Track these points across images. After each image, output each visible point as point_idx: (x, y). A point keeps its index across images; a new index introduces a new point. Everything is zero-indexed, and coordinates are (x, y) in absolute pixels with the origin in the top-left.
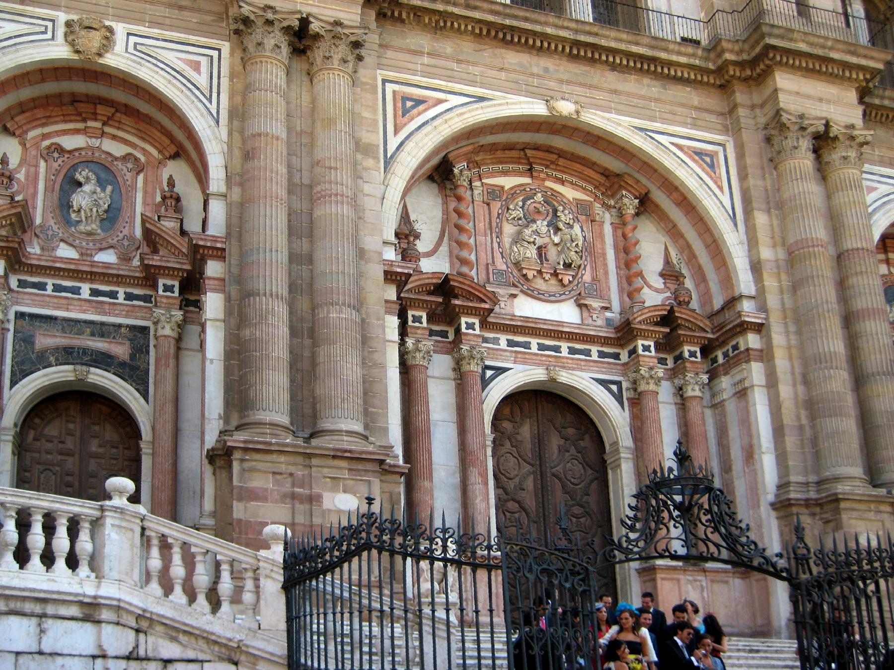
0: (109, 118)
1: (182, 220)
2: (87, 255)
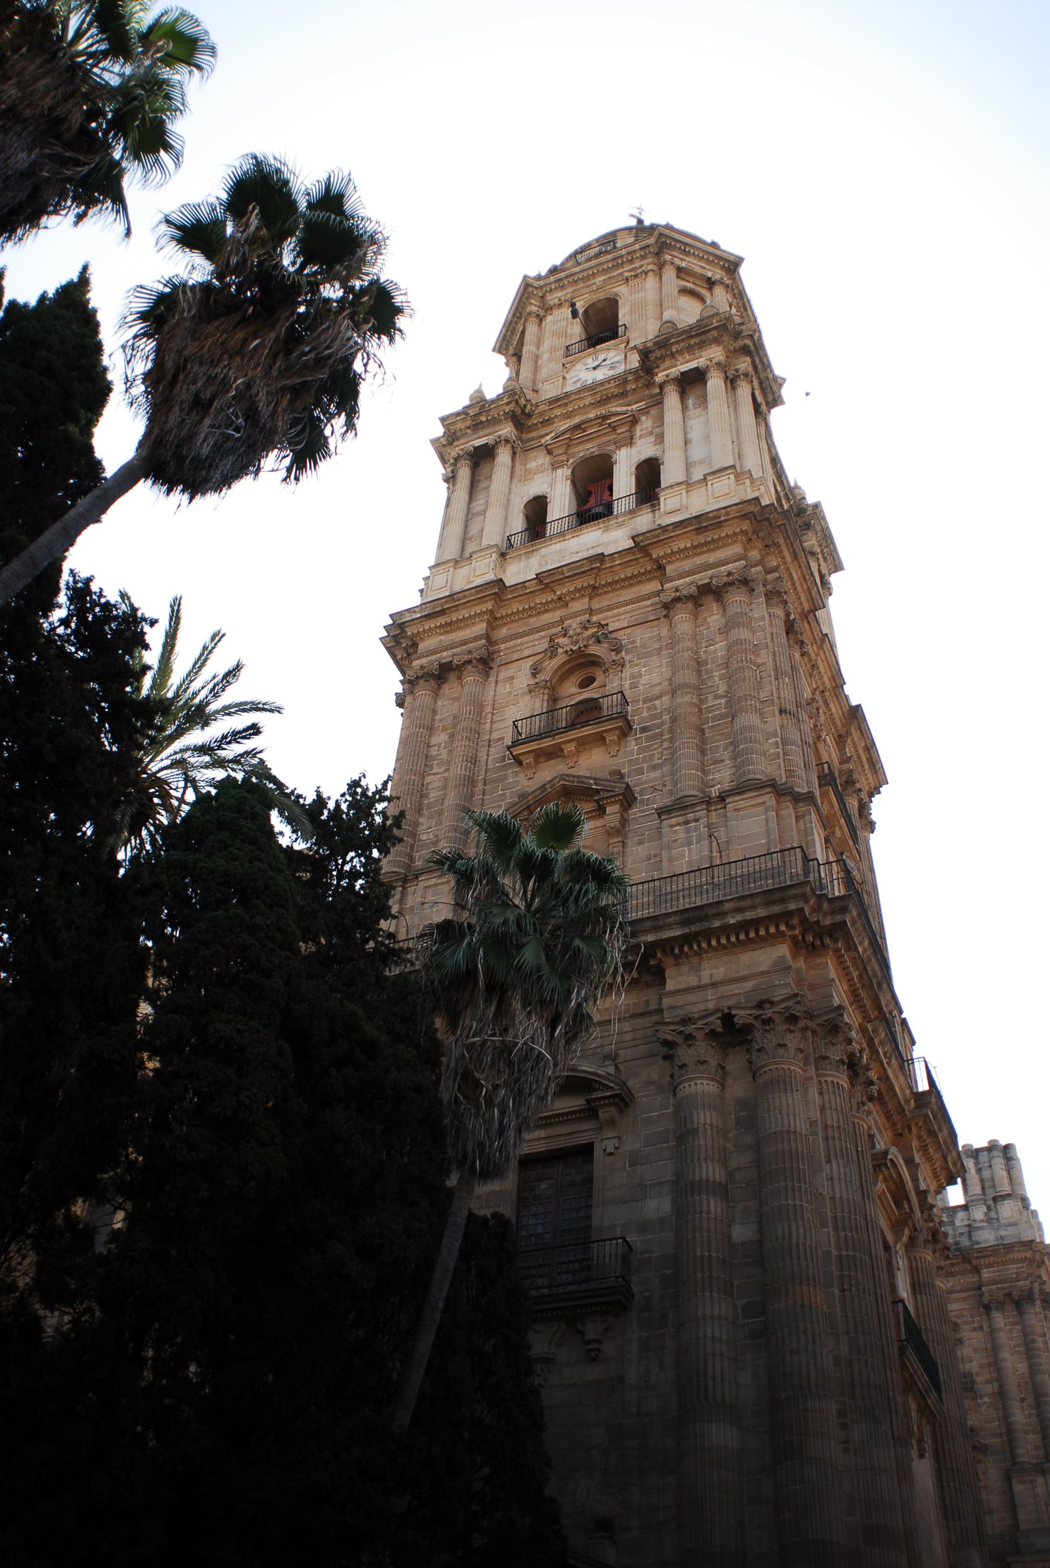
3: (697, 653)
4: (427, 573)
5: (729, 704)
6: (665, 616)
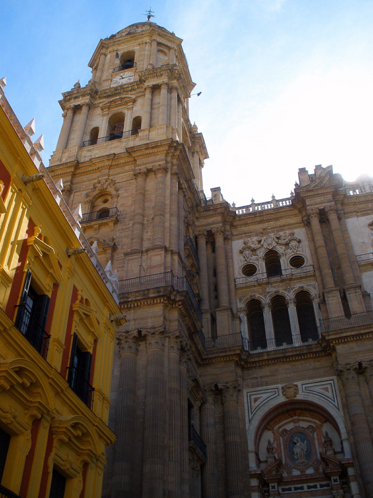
0: (300, 414)
1: (334, 450)
2: (303, 472)
4: (52, 154)
6: (135, 179)
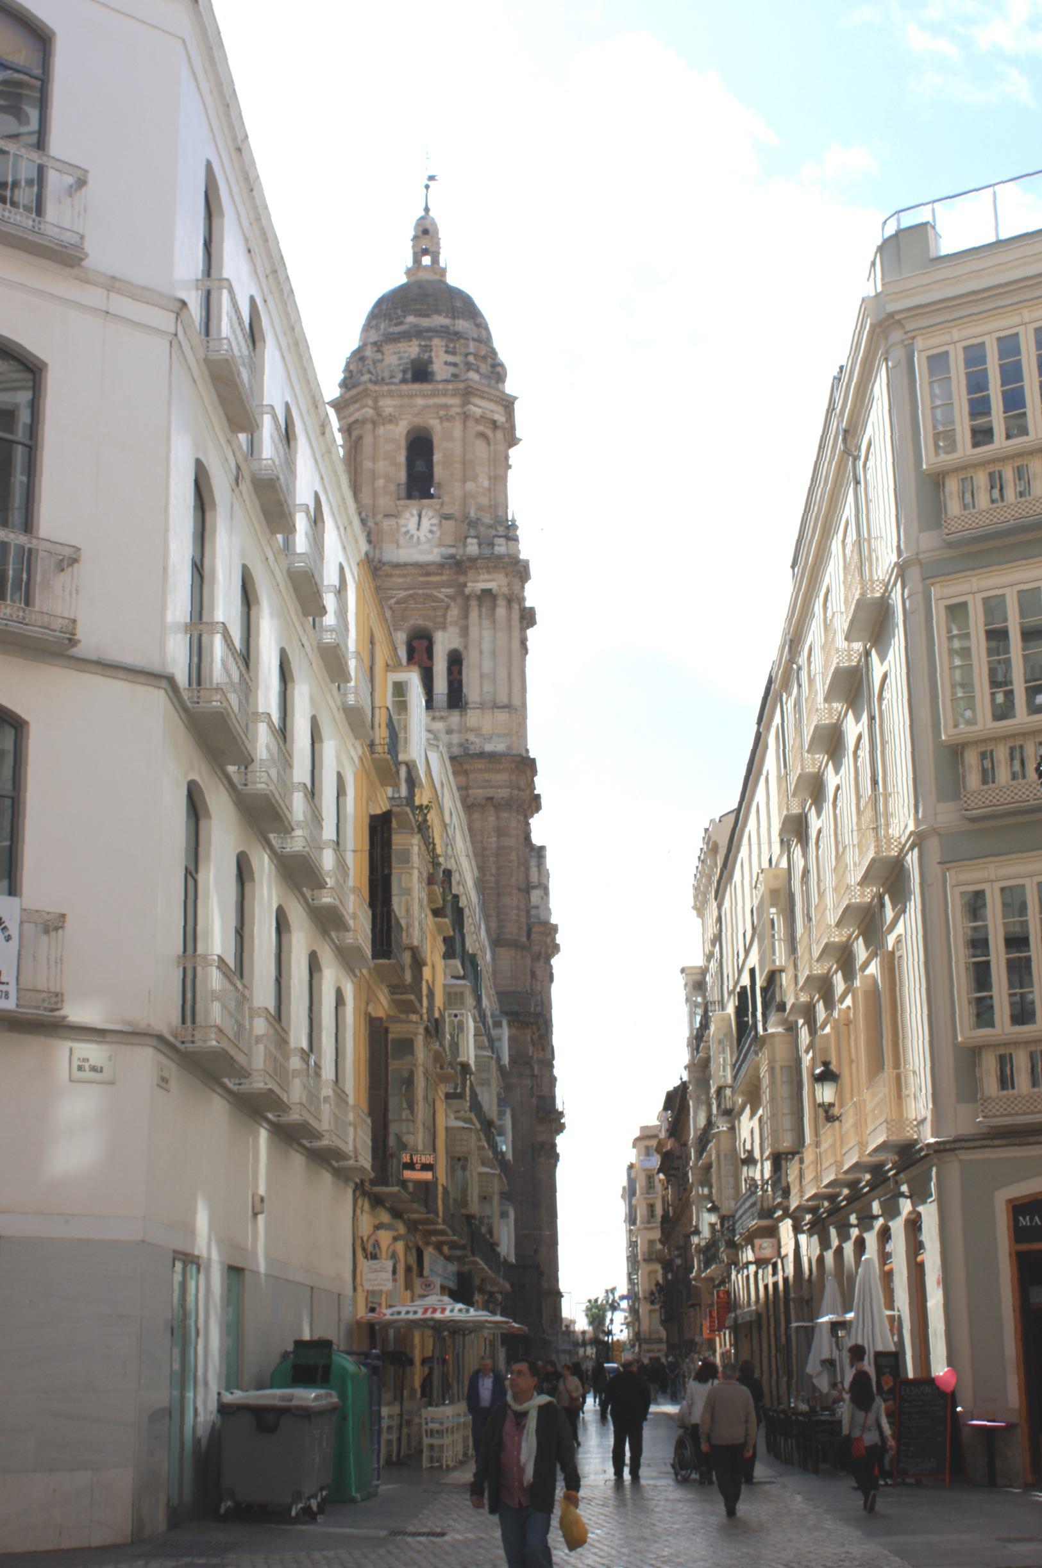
3: (482, 842)
5: (497, 882)
